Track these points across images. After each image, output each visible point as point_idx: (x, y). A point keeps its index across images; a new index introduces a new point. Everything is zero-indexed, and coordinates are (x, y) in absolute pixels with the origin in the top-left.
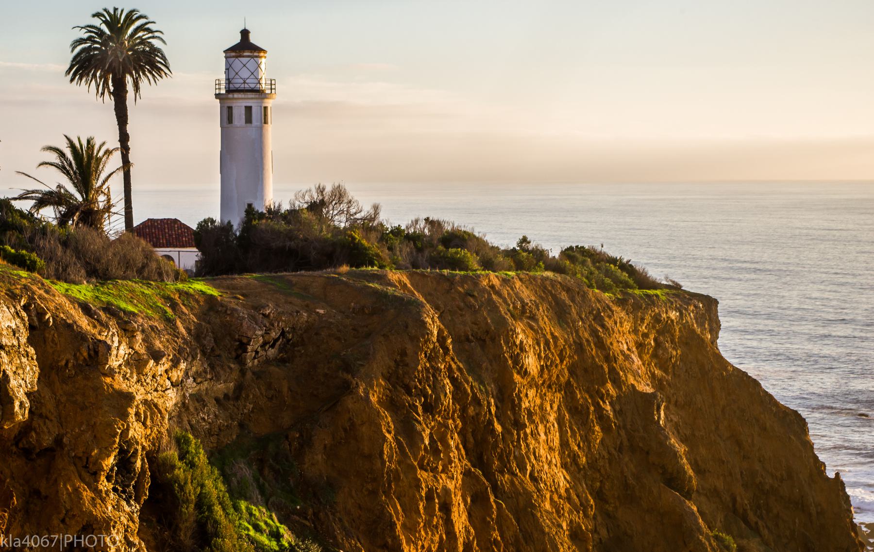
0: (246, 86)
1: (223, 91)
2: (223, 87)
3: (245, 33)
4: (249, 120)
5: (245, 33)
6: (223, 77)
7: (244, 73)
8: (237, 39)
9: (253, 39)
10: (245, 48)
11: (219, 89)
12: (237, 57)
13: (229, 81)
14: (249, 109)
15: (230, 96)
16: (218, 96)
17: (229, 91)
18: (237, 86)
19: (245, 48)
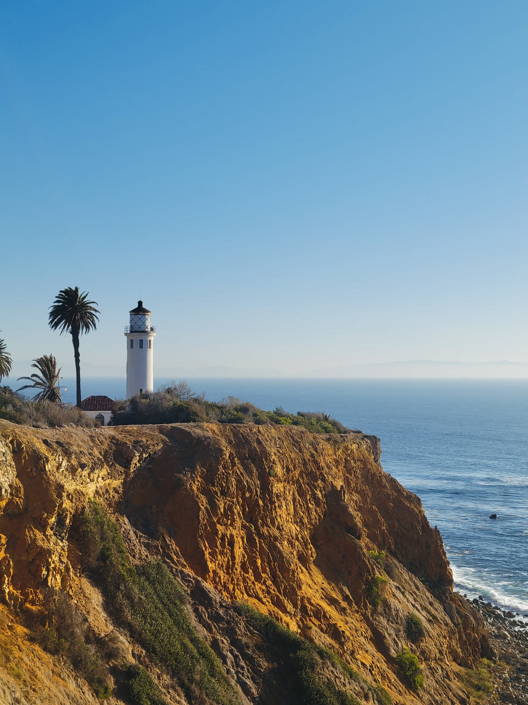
0: (140, 329)
1: (129, 332)
2: (129, 329)
3: (140, 303)
4: (141, 347)
5: (140, 303)
6: (129, 325)
7: (139, 323)
8: (136, 306)
9: (144, 306)
10: (140, 311)
11: (127, 331)
12: (136, 315)
13: (132, 327)
14: (141, 341)
15: (132, 334)
16: (126, 334)
17: (131, 332)
18: (136, 329)
19: (140, 311)
